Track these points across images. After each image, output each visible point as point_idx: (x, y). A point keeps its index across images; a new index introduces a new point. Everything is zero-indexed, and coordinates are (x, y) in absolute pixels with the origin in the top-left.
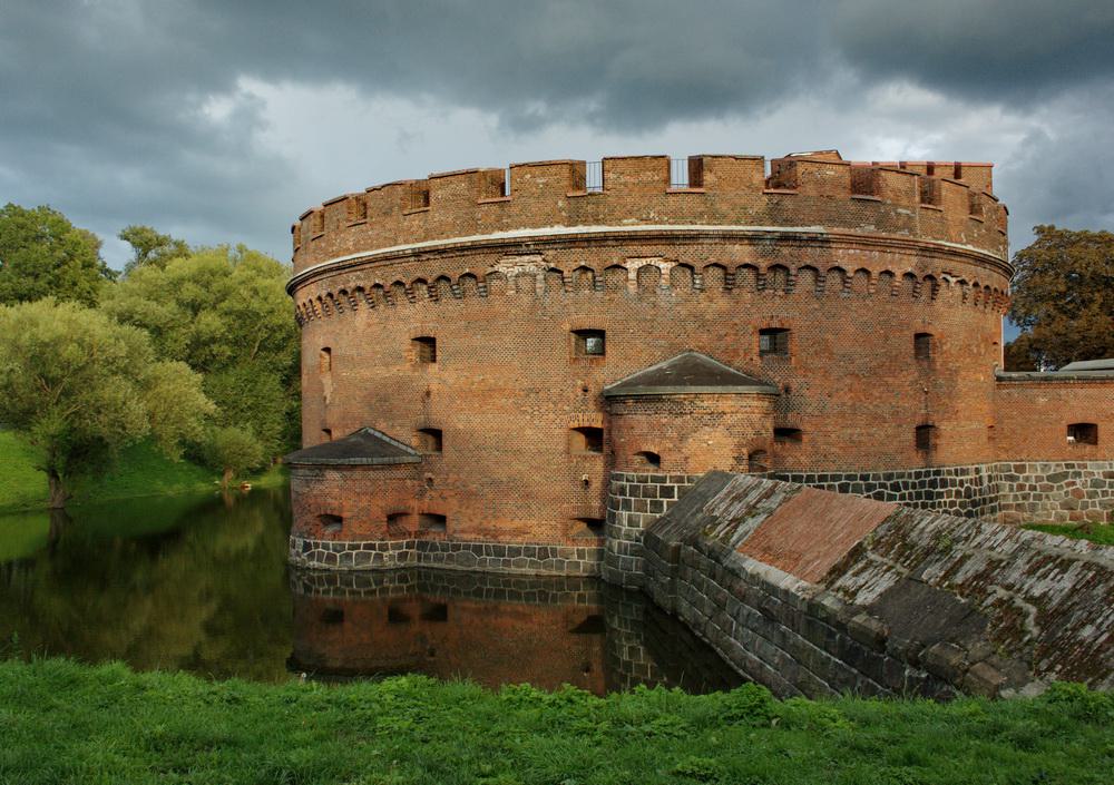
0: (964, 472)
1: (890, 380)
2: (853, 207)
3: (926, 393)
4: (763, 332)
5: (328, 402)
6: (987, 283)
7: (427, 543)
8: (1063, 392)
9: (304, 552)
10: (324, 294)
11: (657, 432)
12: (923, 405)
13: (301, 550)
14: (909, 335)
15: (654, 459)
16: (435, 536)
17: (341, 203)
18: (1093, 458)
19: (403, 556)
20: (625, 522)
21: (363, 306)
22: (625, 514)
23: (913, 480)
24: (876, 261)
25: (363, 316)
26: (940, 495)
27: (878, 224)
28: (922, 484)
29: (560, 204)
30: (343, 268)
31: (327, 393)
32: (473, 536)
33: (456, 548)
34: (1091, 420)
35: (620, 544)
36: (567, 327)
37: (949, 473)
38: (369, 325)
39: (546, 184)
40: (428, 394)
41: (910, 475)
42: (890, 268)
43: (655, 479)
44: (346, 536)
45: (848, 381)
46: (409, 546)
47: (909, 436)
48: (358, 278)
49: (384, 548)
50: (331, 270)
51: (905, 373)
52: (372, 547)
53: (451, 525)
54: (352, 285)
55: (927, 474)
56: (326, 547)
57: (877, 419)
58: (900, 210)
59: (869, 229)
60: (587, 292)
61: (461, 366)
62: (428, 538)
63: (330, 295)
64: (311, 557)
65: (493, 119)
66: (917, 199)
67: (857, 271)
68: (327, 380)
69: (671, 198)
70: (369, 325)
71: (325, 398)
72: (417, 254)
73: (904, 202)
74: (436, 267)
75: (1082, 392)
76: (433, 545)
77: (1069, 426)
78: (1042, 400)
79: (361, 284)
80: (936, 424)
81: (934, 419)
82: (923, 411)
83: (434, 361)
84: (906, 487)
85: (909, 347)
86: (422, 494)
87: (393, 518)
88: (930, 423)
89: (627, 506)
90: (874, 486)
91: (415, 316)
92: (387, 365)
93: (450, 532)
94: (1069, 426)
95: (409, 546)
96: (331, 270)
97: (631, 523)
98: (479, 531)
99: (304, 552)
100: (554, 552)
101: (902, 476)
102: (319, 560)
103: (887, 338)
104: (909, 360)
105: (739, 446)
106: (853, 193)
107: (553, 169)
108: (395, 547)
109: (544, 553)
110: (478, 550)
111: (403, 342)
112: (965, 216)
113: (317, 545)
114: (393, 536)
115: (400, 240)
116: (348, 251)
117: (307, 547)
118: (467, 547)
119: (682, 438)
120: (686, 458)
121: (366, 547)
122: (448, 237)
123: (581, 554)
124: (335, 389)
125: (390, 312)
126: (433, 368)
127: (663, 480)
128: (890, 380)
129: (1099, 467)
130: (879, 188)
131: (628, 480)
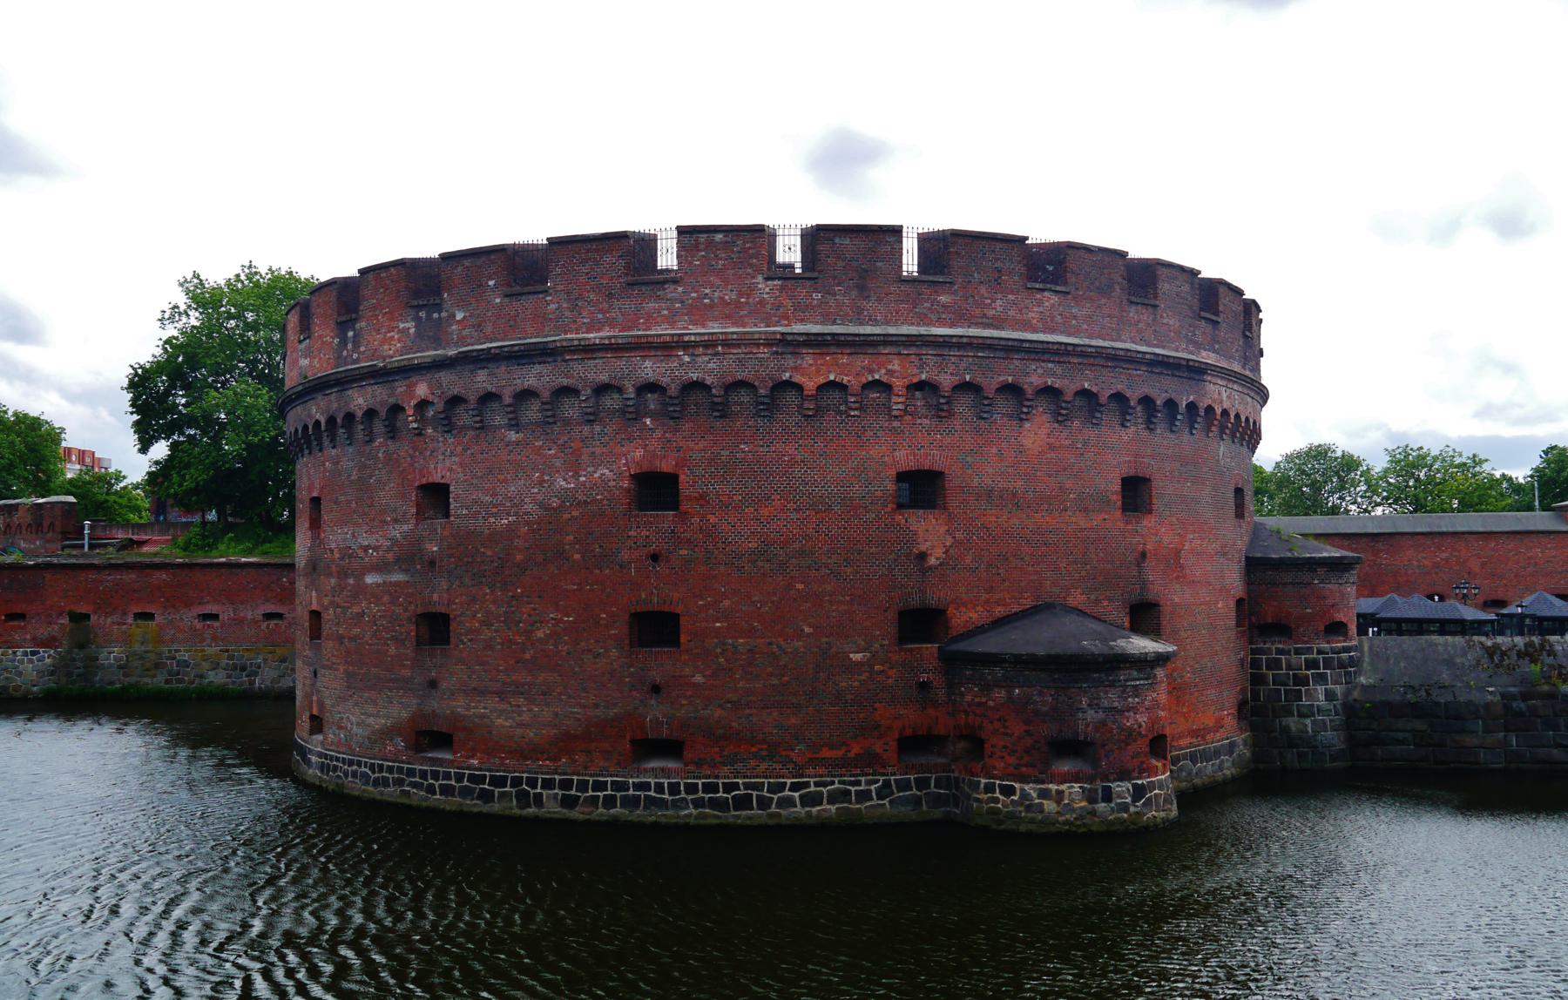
5: (932, 561)
9: (1136, 799)
13: (1129, 800)
17: (999, 246)
20: (1322, 697)
22: (1321, 689)
25: (1037, 432)
35: (1314, 722)
38: (1051, 447)
40: (1143, 555)
48: (1048, 373)
50: (990, 347)
64: (1148, 803)
71: (923, 556)
89: (1321, 679)
91: (1117, 448)
96: (990, 347)
97: (1330, 696)
99: (1136, 799)
116: (1026, 326)
117: (1139, 792)
124: (957, 543)
125: (1090, 433)
126: (1148, 522)
131: (1320, 652)
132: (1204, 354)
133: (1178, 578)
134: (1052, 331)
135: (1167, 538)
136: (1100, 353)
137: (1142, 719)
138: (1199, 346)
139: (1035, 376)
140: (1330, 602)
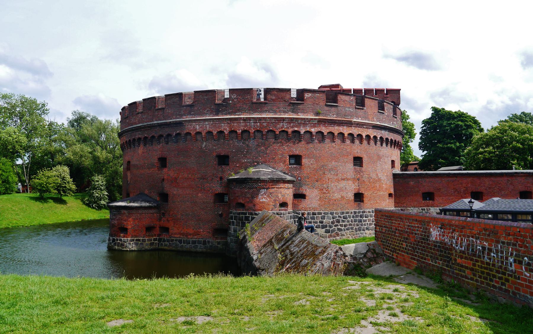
2: (327, 108)
4: (291, 157)
6: (387, 137)
7: (161, 239)
8: (420, 180)
10: (128, 140)
11: (244, 195)
14: (351, 158)
15: (242, 205)
16: (165, 237)
18: (433, 206)
19: (152, 244)
20: (232, 230)
21: (142, 145)
24: (336, 130)
25: (141, 150)
26: (365, 221)
27: (338, 114)
28: (357, 216)
29: (212, 107)
30: (136, 129)
31: (129, 179)
32: (179, 236)
33: (172, 241)
34: (432, 190)
36: (215, 154)
37: (369, 212)
39: (207, 99)
41: (352, 212)
42: (342, 131)
43: (243, 213)
44: (129, 236)
46: (155, 240)
48: (139, 134)
49: (144, 241)
52: (139, 240)
53: (171, 231)
54: (137, 137)
56: (121, 240)
58: (347, 109)
59: (334, 117)
60: (222, 141)
61: (175, 169)
62: (162, 237)
63: (130, 140)
64: (115, 244)
65: (59, 114)
66: (354, 104)
67: (328, 133)
68: (129, 174)
69: (254, 105)
70: (143, 153)
72: (160, 125)
73: (348, 106)
74: (167, 131)
75: (428, 180)
76: (164, 239)
77: (423, 193)
78: (412, 183)
79: (140, 136)
81: (362, 191)
83: (166, 167)
84: (350, 217)
86: (160, 220)
87: (149, 229)
88: (360, 192)
90: (336, 217)
91: (157, 150)
92: (149, 168)
93: (170, 234)
94: (423, 193)
95: (155, 240)
98: (181, 234)
100: (209, 242)
101: (347, 213)
102: (118, 246)
105: (275, 200)
106: (327, 102)
107: (210, 94)
108: (148, 240)
109: (205, 243)
110: (180, 241)
111: (155, 160)
112: (376, 110)
113: (117, 240)
114: (149, 236)
115: (154, 120)
116: (136, 124)
118: (176, 240)
119: (253, 197)
120: (254, 205)
121: (136, 240)
122: (171, 119)
123: (219, 243)
126: (165, 170)
127: (245, 214)
129: (435, 209)
130: (337, 100)
132: (184, 117)
133: (176, 186)
134: (139, 123)
135: (172, 174)
136: (144, 127)
137: (116, 222)
138: (181, 116)
139: (138, 135)
140: (237, 195)
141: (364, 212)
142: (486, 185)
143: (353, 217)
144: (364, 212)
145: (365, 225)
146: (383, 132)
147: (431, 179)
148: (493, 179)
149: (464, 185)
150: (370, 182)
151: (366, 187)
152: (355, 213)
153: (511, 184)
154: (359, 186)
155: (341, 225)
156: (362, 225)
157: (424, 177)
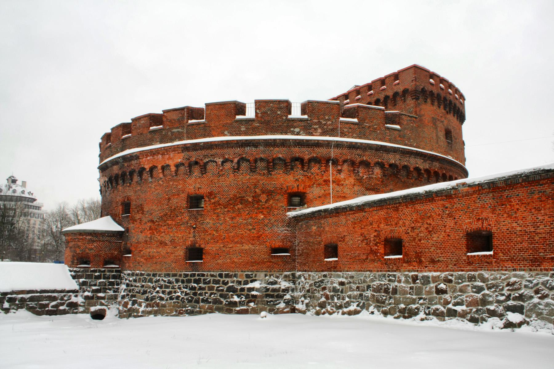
0: (231, 277)
1: (169, 222)
3: (194, 228)
8: (322, 222)
12: (192, 235)
14: (183, 196)
23: (182, 278)
26: (204, 289)
37: (212, 276)
41: (180, 275)
45: (149, 224)
47: (181, 252)
51: (180, 218)
55: (194, 275)
57: (162, 244)
75: (330, 220)
80: (202, 246)
82: (191, 239)
85: (184, 204)
103: (169, 199)
104: (183, 211)
105: (73, 256)
128: (169, 222)
141: (203, 275)
142: (407, 223)
143: (183, 282)
144: (203, 275)
145: (201, 294)
146: (247, 149)
147: (335, 219)
148: (418, 207)
149: (375, 226)
150: (217, 231)
151: (209, 237)
152: (186, 275)
153: (450, 215)
154: (194, 237)
155: (163, 292)
156: (195, 294)
157: (325, 217)
